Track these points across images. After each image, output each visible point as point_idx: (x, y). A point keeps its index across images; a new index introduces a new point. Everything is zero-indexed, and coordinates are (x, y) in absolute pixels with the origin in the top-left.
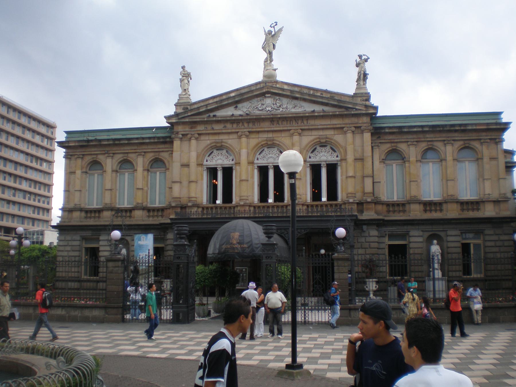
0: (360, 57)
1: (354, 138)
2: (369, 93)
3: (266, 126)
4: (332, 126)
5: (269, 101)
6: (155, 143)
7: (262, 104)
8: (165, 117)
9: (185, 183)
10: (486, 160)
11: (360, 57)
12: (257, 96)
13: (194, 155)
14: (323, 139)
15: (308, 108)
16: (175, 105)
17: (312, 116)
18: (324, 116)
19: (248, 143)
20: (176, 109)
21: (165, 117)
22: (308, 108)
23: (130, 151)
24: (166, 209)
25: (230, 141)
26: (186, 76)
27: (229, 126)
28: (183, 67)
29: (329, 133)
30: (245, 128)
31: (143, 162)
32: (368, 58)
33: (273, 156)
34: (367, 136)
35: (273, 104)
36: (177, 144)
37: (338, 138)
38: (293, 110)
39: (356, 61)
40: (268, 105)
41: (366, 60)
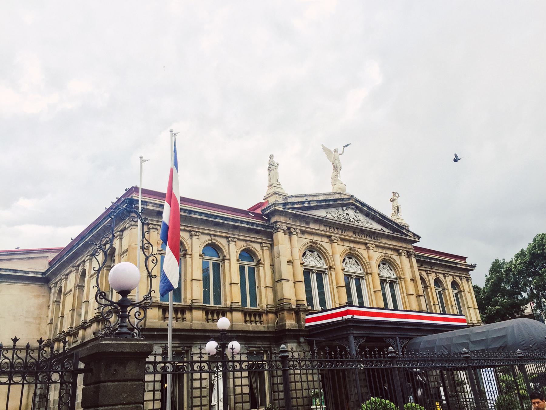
0: (394, 193)
3: (350, 235)
4: (392, 247)
5: (351, 213)
6: (249, 230)
9: (291, 282)
10: (466, 293)
12: (342, 205)
13: (296, 251)
14: (388, 257)
15: (376, 227)
17: (372, 234)
18: (388, 237)
22: (376, 227)
23: (220, 234)
24: (267, 312)
25: (323, 244)
27: (323, 228)
28: (271, 157)
29: (389, 252)
30: (336, 234)
34: (414, 260)
37: (396, 258)
38: (366, 225)
40: (353, 216)
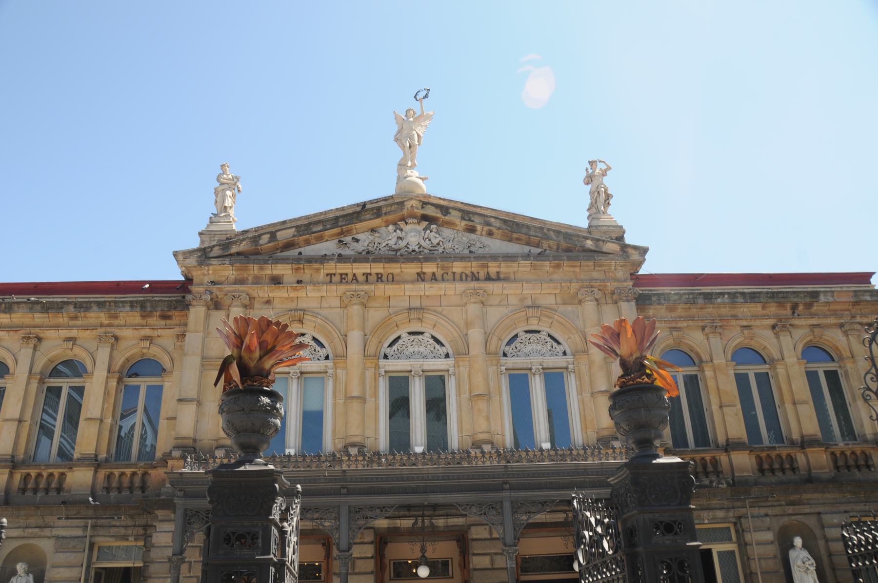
1: (599, 312)
2: (621, 227)
7: (399, 238)
8: (175, 254)
11: (592, 163)
16: (200, 234)
19: (364, 319)
20: (202, 242)
21: (175, 254)
26: (226, 185)
31: (111, 358)
32: (609, 168)
33: (422, 349)
35: (424, 239)
36: (197, 313)
39: (587, 169)
41: (604, 173)
